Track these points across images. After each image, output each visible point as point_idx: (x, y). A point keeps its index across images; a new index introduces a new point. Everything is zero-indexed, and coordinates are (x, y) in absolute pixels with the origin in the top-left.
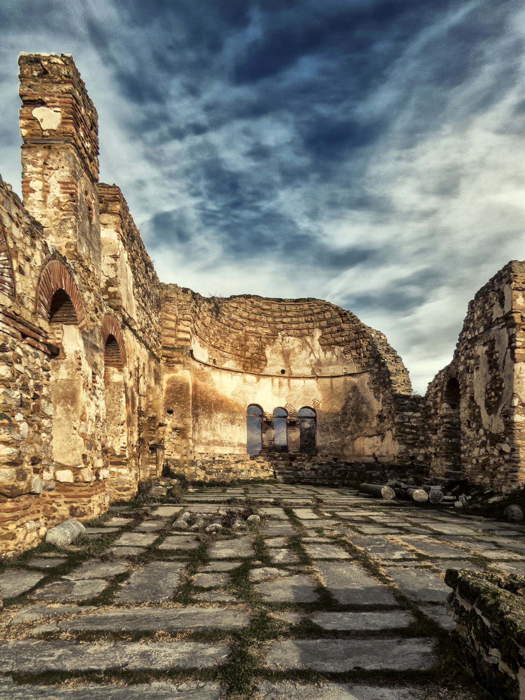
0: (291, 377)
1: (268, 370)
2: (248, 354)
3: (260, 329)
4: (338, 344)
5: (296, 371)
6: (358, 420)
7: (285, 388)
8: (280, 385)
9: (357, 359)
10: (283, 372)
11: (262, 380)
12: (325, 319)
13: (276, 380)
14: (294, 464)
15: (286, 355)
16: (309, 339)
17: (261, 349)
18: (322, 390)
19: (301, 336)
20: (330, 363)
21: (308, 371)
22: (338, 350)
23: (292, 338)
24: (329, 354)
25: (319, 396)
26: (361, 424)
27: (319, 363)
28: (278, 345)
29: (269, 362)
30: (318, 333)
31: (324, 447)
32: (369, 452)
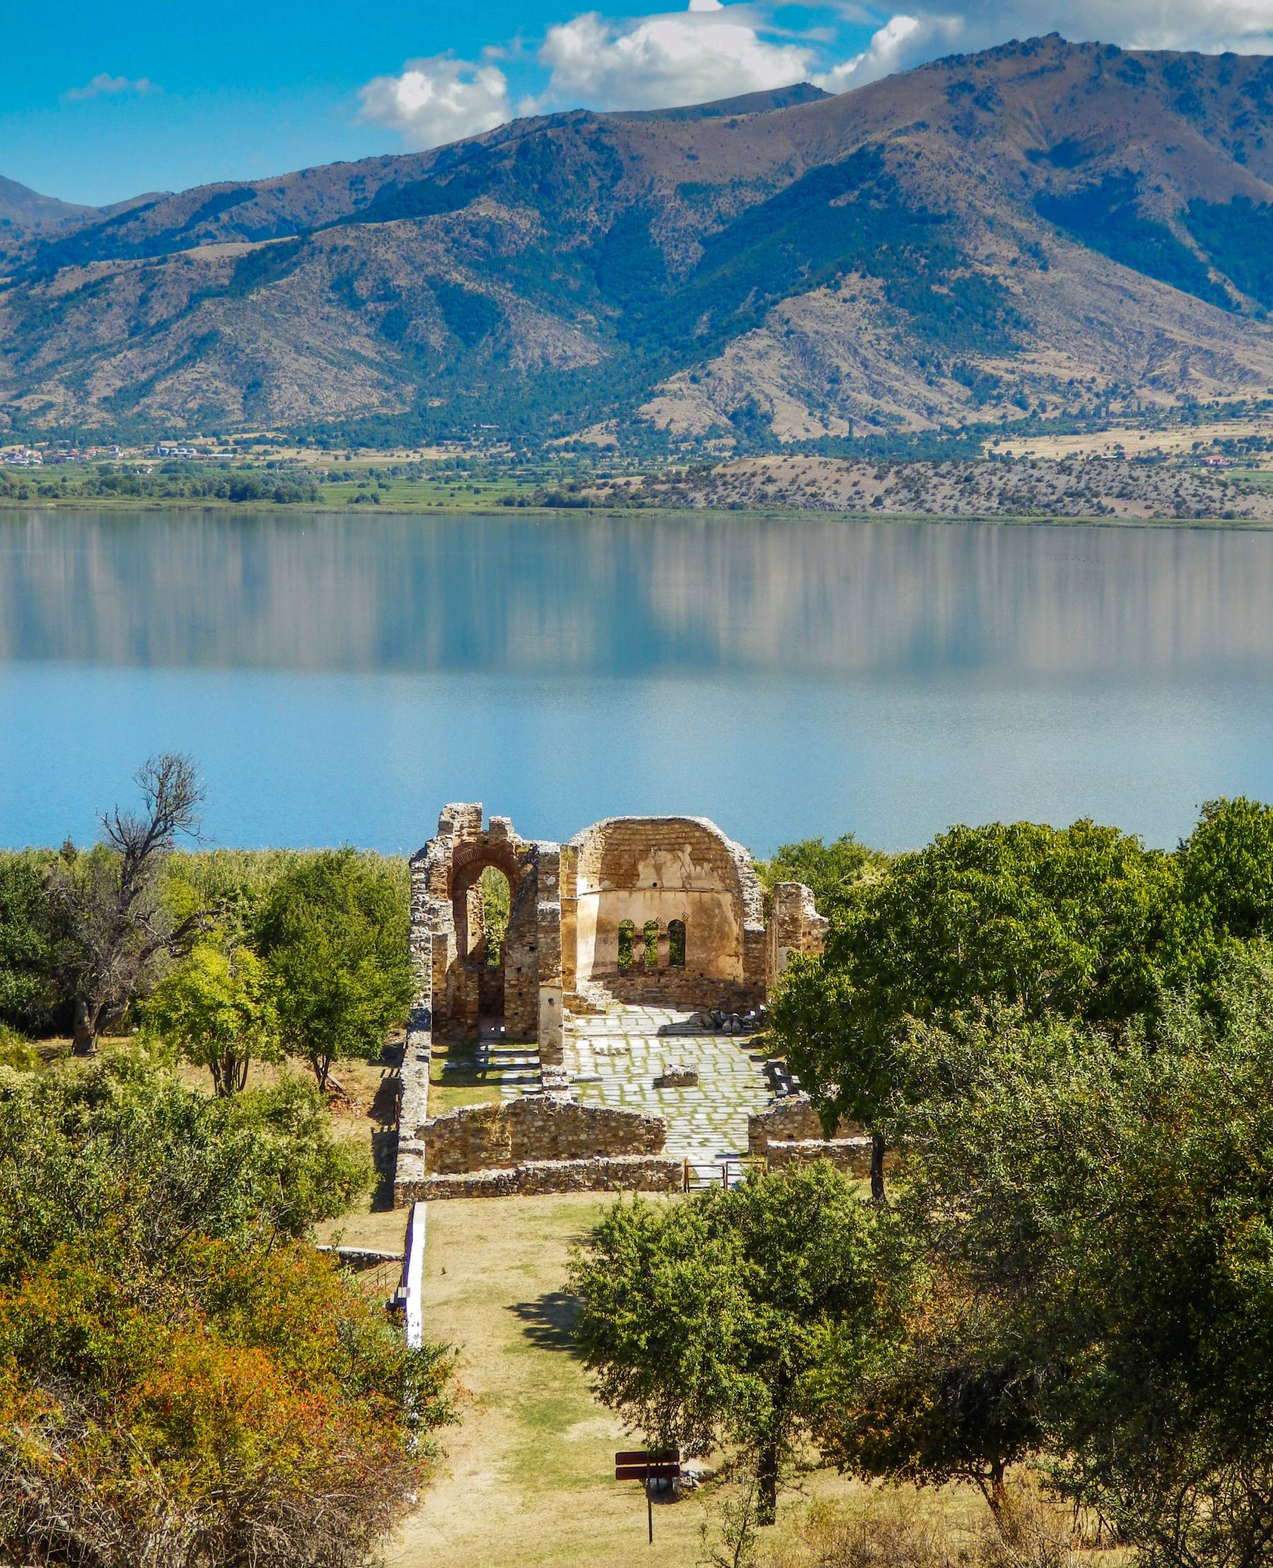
0: (662, 889)
1: (639, 884)
2: (622, 872)
3: (633, 847)
4: (708, 860)
5: (666, 884)
6: (722, 938)
7: (656, 901)
8: (652, 897)
9: (722, 879)
10: (655, 885)
11: (635, 895)
12: (694, 837)
13: (648, 894)
14: (662, 980)
15: (658, 868)
16: (680, 854)
17: (635, 865)
18: (693, 904)
19: (672, 851)
20: (699, 878)
21: (679, 884)
22: (707, 866)
23: (664, 853)
24: (698, 868)
25: (689, 910)
26: (724, 942)
27: (689, 877)
28: (651, 861)
29: (642, 876)
30: (688, 849)
31: (691, 962)
32: (728, 971)
